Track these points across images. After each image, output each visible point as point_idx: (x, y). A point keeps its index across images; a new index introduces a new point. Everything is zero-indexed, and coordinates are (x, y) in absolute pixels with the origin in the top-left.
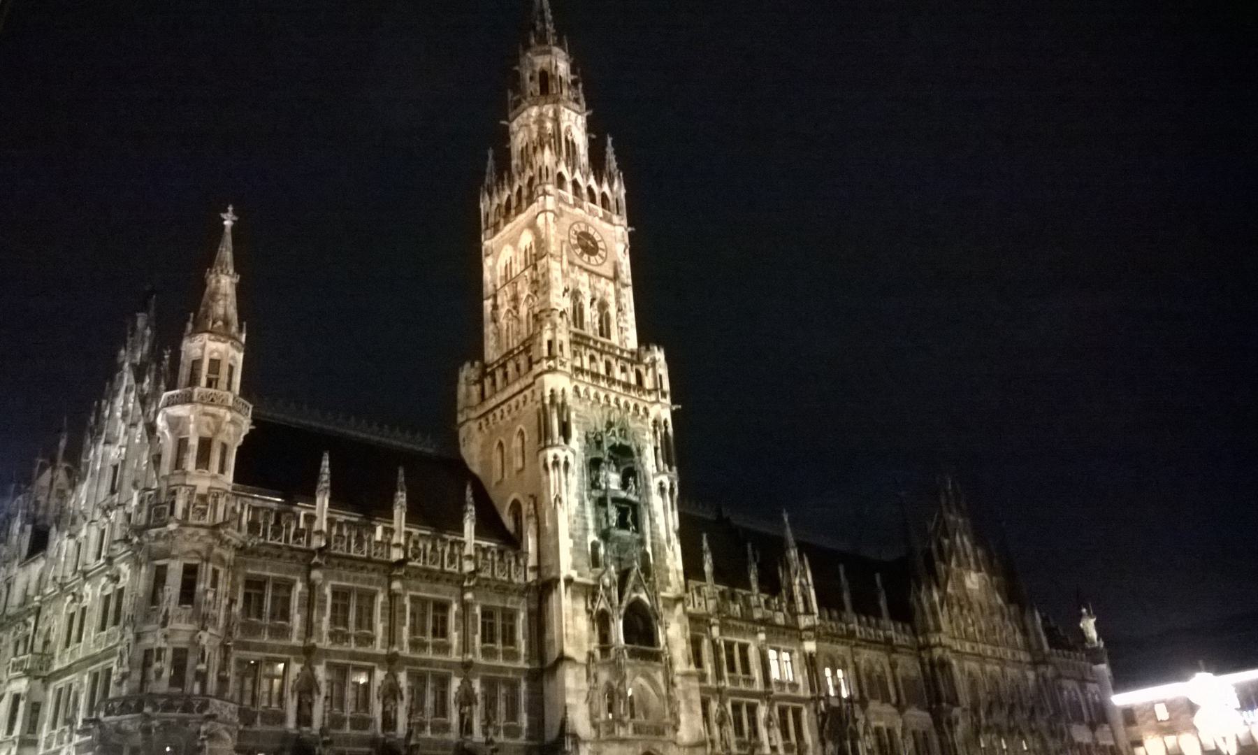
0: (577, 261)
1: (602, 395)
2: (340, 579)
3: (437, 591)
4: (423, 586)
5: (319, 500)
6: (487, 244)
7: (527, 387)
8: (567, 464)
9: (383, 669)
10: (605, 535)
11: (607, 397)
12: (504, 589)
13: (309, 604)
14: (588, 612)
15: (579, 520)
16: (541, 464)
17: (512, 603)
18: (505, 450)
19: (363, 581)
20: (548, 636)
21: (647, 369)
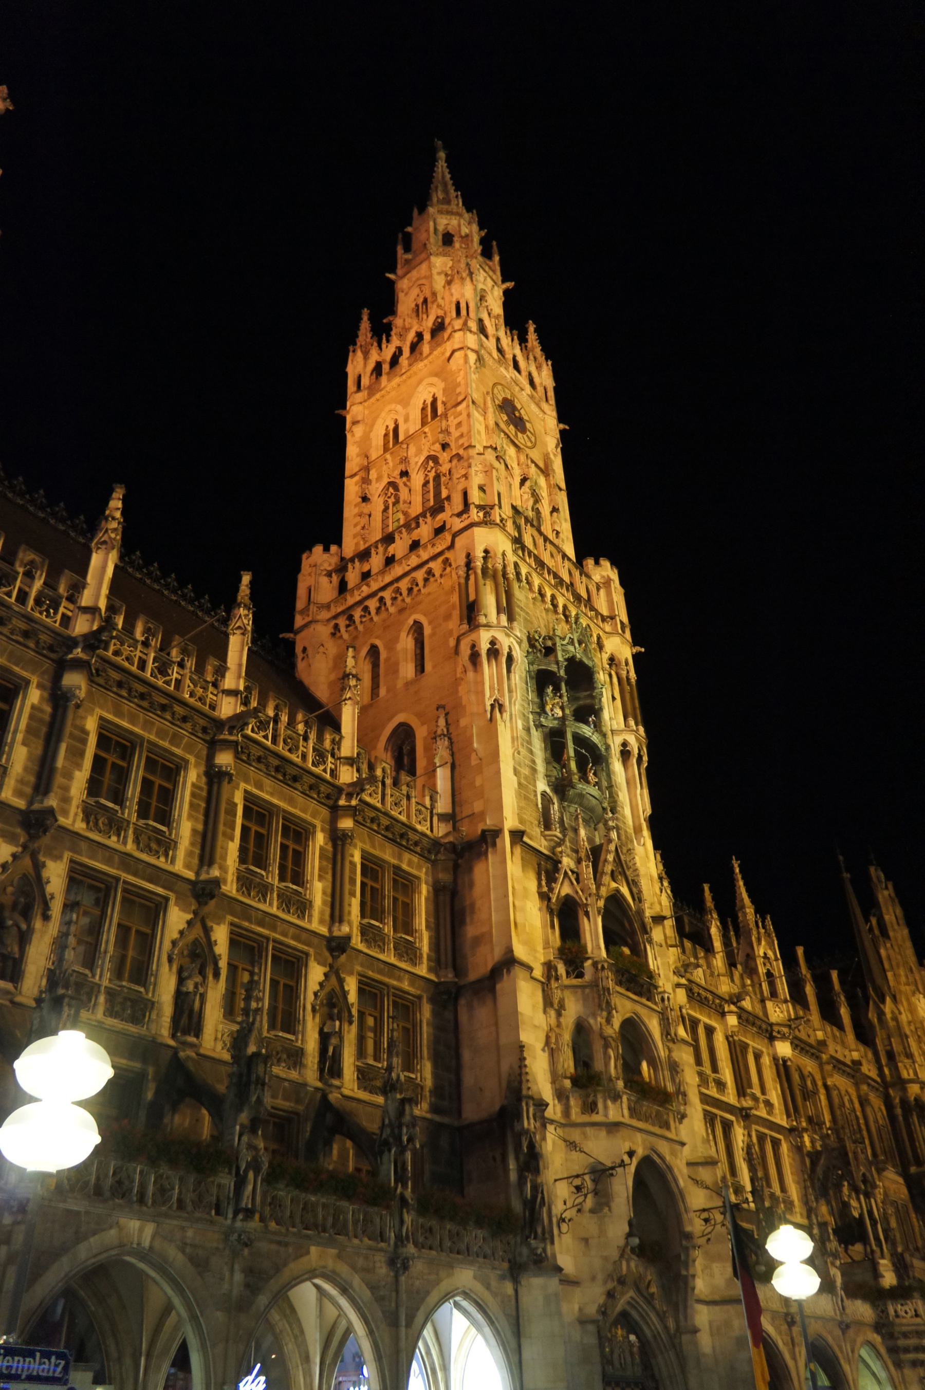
0: (503, 426)
1: (549, 593)
2: (118, 713)
3: (291, 801)
4: (267, 782)
5: (96, 559)
6: (356, 408)
7: (434, 558)
8: (510, 659)
9: (184, 910)
10: (561, 787)
11: (553, 597)
12: (399, 835)
13: (53, 730)
14: (544, 897)
15: (523, 751)
16: (465, 650)
17: (410, 864)
18: (383, 655)
19: (161, 734)
20: (471, 931)
21: (598, 589)
